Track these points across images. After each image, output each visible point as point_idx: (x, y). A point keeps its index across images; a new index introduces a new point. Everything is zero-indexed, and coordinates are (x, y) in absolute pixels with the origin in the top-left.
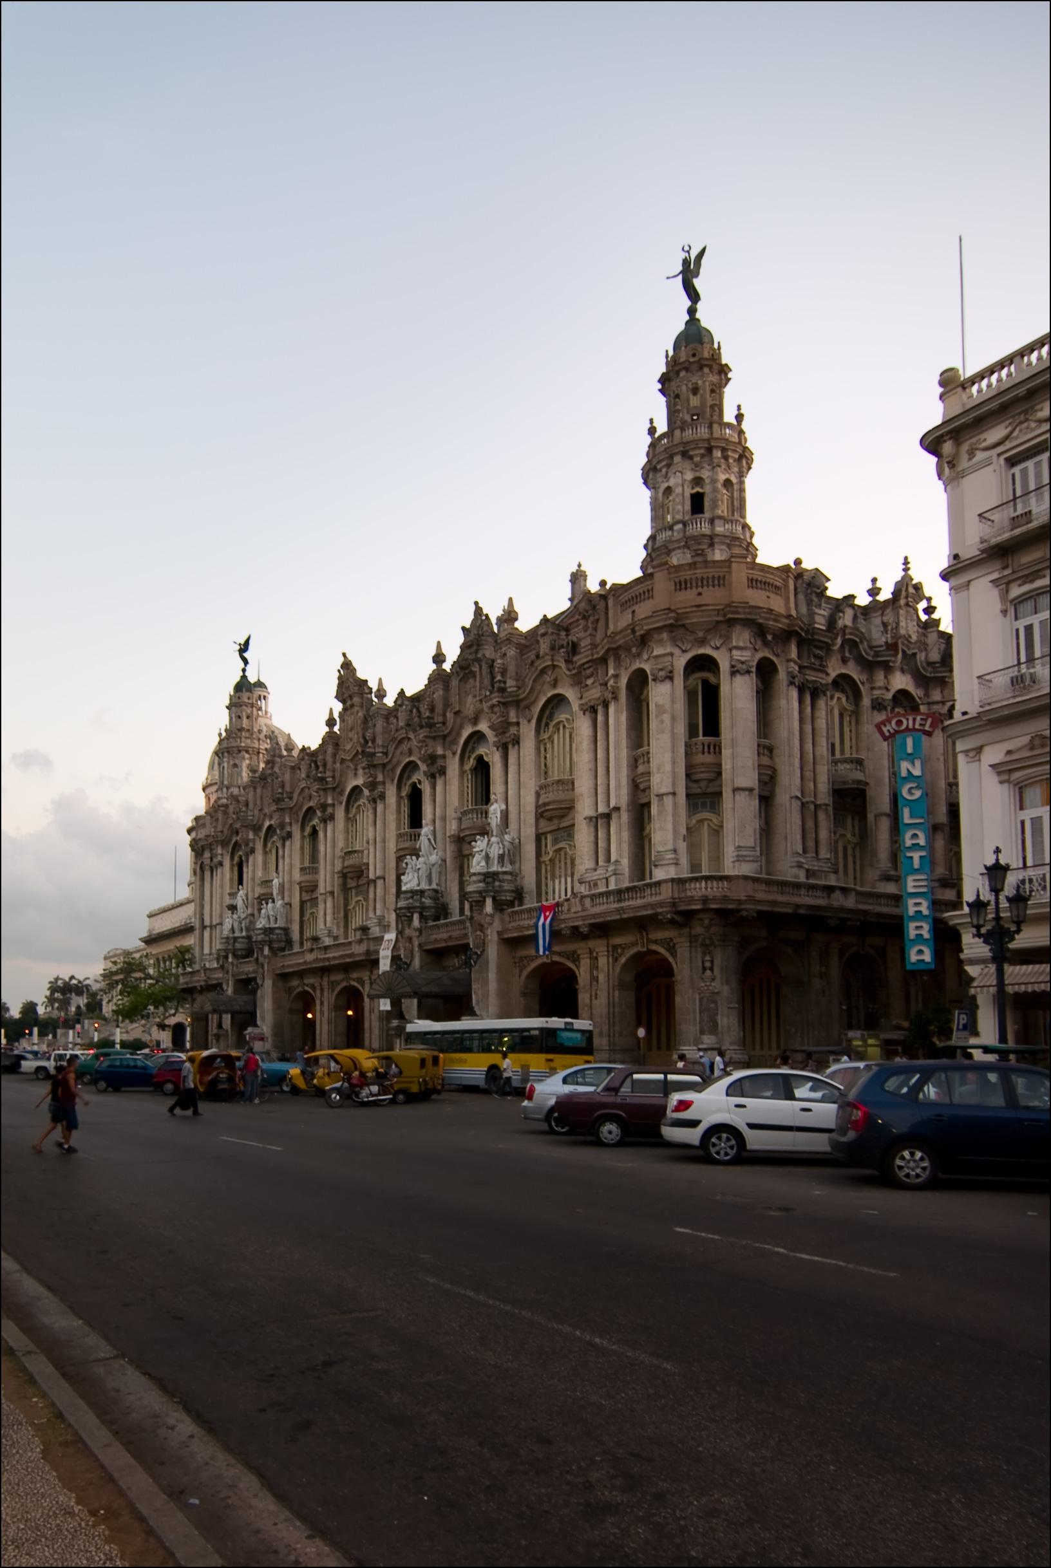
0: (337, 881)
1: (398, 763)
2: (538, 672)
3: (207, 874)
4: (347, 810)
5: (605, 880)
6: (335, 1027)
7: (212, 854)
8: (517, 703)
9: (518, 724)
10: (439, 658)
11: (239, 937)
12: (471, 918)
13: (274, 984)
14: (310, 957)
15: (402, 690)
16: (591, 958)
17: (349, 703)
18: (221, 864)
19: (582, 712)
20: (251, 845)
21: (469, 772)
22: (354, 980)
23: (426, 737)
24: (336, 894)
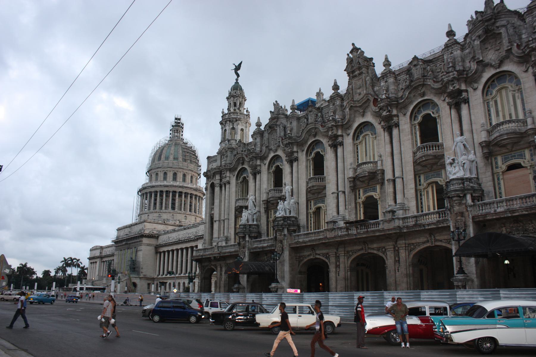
1: (411, 103)
3: (217, 189)
7: (221, 177)
10: (451, 33)
13: (290, 255)
14: (329, 235)
15: (415, 56)
17: (357, 73)
18: (229, 183)
19: (382, 130)
20: (258, 168)
22: (373, 249)
23: (454, 78)
24: (346, 193)
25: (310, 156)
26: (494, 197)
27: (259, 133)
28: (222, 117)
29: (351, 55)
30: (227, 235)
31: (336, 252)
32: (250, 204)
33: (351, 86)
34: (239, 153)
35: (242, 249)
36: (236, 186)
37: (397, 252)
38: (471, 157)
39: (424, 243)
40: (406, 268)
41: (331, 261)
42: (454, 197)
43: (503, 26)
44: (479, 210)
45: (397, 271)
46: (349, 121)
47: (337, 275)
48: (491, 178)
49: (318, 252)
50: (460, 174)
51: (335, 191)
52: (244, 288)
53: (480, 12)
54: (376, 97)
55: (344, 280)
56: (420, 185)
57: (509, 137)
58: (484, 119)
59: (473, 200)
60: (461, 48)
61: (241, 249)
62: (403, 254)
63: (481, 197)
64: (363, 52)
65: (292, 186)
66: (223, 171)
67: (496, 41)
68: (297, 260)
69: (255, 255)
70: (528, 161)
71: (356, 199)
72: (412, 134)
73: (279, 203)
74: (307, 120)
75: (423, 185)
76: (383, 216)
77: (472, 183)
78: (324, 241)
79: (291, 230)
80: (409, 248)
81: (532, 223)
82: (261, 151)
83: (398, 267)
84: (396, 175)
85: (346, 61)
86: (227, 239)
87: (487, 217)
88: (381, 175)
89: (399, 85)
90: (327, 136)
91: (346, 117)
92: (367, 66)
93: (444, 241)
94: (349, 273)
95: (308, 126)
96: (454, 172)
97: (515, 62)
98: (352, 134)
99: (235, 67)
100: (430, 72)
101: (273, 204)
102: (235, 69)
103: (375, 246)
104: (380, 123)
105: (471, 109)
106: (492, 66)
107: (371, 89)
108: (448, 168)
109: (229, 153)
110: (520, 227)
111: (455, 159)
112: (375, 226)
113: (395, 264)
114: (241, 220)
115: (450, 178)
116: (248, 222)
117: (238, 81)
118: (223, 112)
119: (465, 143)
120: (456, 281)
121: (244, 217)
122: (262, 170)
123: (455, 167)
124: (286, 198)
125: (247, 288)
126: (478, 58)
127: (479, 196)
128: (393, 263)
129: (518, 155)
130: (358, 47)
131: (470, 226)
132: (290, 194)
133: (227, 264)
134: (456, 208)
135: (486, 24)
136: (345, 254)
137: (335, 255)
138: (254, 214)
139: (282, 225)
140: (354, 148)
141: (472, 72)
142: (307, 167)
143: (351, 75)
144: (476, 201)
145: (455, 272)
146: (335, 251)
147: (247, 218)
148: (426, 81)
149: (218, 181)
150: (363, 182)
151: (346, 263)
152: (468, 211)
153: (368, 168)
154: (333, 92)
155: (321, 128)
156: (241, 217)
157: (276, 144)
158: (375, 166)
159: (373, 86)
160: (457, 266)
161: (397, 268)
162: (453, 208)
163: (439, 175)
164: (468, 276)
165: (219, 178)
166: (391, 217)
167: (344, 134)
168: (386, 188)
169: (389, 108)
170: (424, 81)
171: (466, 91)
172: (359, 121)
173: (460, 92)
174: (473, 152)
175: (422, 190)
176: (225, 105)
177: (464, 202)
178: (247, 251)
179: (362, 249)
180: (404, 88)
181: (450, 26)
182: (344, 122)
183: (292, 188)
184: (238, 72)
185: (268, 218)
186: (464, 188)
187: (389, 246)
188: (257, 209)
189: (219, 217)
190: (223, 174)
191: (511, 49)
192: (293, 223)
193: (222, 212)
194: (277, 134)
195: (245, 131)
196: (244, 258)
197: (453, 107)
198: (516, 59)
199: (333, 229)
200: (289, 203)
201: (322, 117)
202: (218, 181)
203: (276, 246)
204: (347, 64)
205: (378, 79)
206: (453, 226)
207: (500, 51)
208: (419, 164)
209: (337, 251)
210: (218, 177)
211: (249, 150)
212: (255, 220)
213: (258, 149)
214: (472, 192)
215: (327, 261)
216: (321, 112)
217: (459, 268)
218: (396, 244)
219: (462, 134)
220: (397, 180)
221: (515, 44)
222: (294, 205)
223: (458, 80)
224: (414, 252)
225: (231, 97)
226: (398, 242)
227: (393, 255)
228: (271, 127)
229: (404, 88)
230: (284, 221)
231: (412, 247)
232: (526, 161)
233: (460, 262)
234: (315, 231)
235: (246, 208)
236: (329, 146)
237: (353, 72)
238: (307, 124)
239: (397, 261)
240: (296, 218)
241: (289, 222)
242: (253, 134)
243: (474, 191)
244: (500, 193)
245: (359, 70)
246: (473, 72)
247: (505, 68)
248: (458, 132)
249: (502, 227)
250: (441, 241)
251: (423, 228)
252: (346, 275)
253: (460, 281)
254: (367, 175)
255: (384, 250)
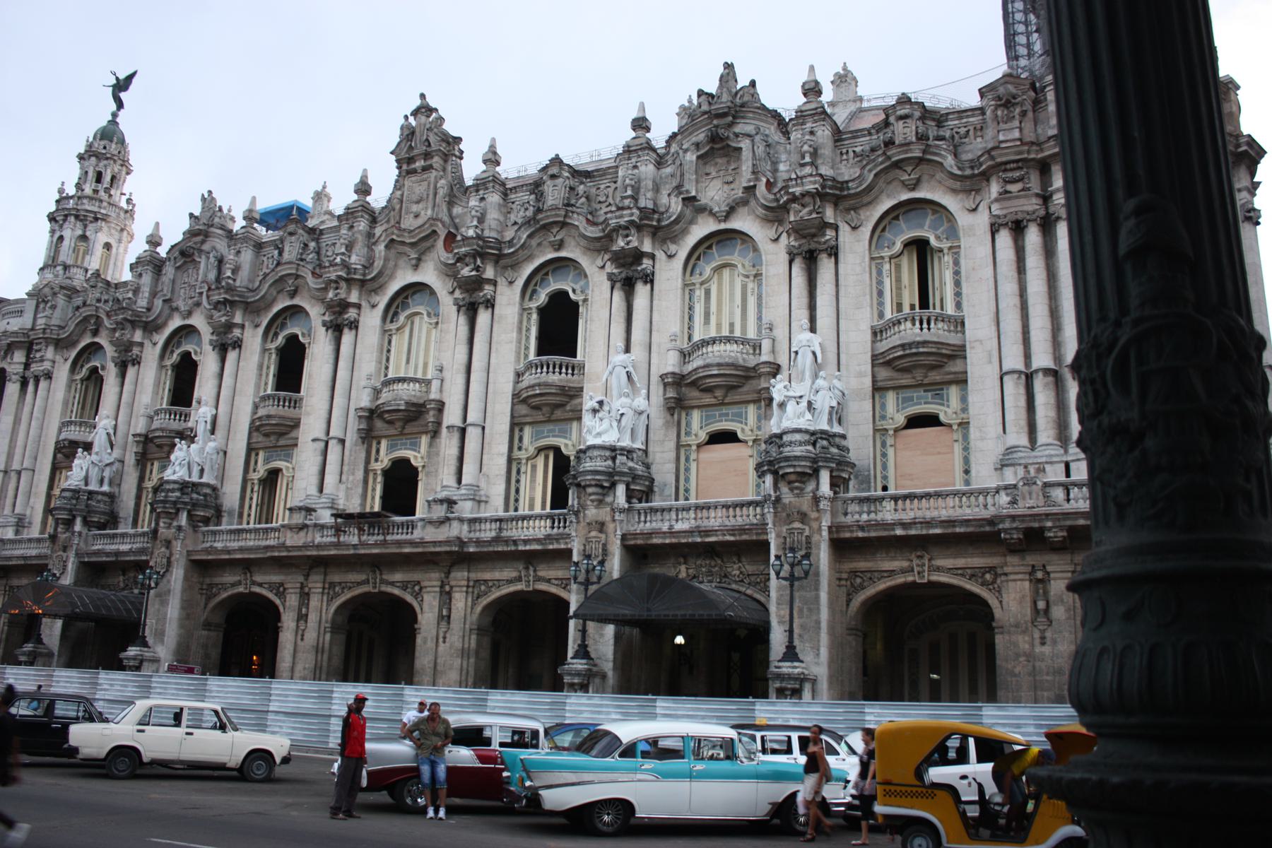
0: (354, 425)
1: (530, 258)
2: (887, 164)
4: (384, 319)
5: (1063, 466)
6: (330, 659)
7: (28, 357)
8: (837, 201)
9: (836, 228)
10: (641, 124)
11: (97, 493)
12: (778, 500)
13: (186, 578)
14: (292, 539)
15: (557, 155)
16: (1031, 581)
17: (419, 164)
18: (49, 376)
19: (455, 308)
20: (136, 350)
21: (169, 368)
22: (392, 584)
23: (632, 222)
24: (347, 444)
25: (272, 341)
26: (673, 497)
27: (151, 264)
28: (57, 201)
29: (412, 120)
30: (22, 512)
31: (302, 583)
32: (99, 438)
33: (399, 193)
34: (88, 302)
35: (61, 553)
36: (69, 387)
37: (446, 596)
38: (640, 402)
39: (510, 582)
40: (464, 636)
41: (287, 604)
42: (590, 486)
43: (749, 136)
44: (639, 522)
45: (441, 640)
46: (380, 274)
47: (299, 637)
48: (673, 455)
49: (258, 578)
50: (610, 438)
51: (322, 436)
52: (50, 655)
53: (707, 94)
54: (452, 230)
55: (314, 653)
56: (520, 449)
57: (722, 372)
58: (678, 325)
59: (629, 498)
60: (656, 161)
61: (56, 552)
62: (460, 602)
63: (647, 494)
64: (441, 119)
65: (217, 409)
66: (37, 344)
67: (728, 162)
68: (202, 594)
69: (94, 571)
70: (752, 431)
71: (367, 462)
72: (520, 329)
73: (175, 445)
74: (280, 254)
75: (526, 450)
76: (426, 510)
77: (632, 460)
78: (276, 554)
79: (198, 518)
80: (476, 590)
81: (740, 561)
82: (149, 310)
83: (446, 632)
84: (469, 420)
85: (398, 132)
86: (21, 524)
87: (652, 538)
88: (436, 412)
89: (509, 213)
90: (322, 301)
91: (376, 264)
92: (446, 155)
93: (556, 582)
94: (328, 636)
95: (279, 268)
96: (598, 430)
97: (758, 216)
98: (382, 306)
99: (115, 82)
100: (583, 200)
101: (160, 446)
102: (114, 86)
103: (398, 577)
104: (452, 293)
105: (655, 296)
106: (712, 213)
107: (445, 210)
108: (587, 419)
109: (61, 300)
110: (715, 566)
111: (605, 402)
112: (405, 531)
113: (438, 624)
114: (67, 478)
115: (589, 443)
116: (86, 484)
117: (118, 120)
118: (61, 191)
119: (631, 369)
120: (570, 674)
121: (79, 470)
122: (143, 356)
123: (601, 420)
124: (195, 436)
125: (59, 656)
126: (687, 191)
127: (643, 492)
128: (436, 622)
129: (735, 415)
130: (432, 103)
131: (614, 555)
132: (209, 427)
133: (11, 587)
134: (592, 513)
135: (715, 122)
136: (324, 588)
137: (298, 590)
138: (107, 465)
139: (175, 503)
140: (383, 339)
141: (670, 217)
142: (260, 367)
143: (405, 167)
144: (635, 500)
145: (570, 653)
146: (301, 579)
147: (84, 473)
148: (570, 218)
149: (17, 366)
150: (390, 422)
151: (324, 611)
152: (614, 521)
153: (408, 392)
154: (355, 197)
155: (310, 279)
156: (70, 468)
157: (191, 298)
158: (424, 389)
159: (451, 204)
160: (575, 641)
161: (441, 635)
162: (585, 509)
163: (565, 432)
164: (595, 665)
165: (23, 360)
166: (443, 514)
167: (364, 304)
168: (443, 445)
169: (479, 262)
170: (566, 216)
171: (652, 257)
172: (405, 277)
173: (638, 256)
174: (644, 392)
175: (524, 461)
176: (69, 175)
177: (609, 499)
178: (72, 559)
179: (366, 582)
180: (520, 221)
181: (642, 107)
182: (369, 274)
183: (214, 412)
184: (123, 95)
185: (141, 479)
186: (614, 469)
187: (431, 580)
188: (117, 453)
189: (7, 463)
190: (37, 351)
191: (755, 186)
192: (205, 500)
193: (18, 451)
194: (198, 274)
195: (114, 250)
196: (63, 577)
197: (618, 285)
198: (760, 211)
199: (304, 527)
200: (202, 450)
201: (318, 253)
202: (20, 369)
203: (152, 553)
204: (398, 140)
205: (466, 189)
206: (579, 550)
207: (732, 186)
208: (524, 401)
209: (306, 580)
210: (19, 357)
211: (118, 300)
212: (106, 481)
213: (142, 303)
214: (630, 479)
215: (278, 602)
216: (317, 240)
217: (579, 645)
218: (447, 577)
219: (627, 350)
220: (470, 430)
221: (764, 180)
222: (214, 457)
223: (639, 228)
224: (485, 601)
225: (90, 156)
226: (453, 575)
227: (436, 603)
228: (186, 253)
229: (520, 221)
230: (183, 494)
231: (483, 588)
232: (747, 429)
233: (584, 631)
234: (258, 526)
235: (88, 447)
236: (324, 324)
237: (411, 160)
238: (278, 264)
239: (445, 619)
240: (214, 489)
241: (195, 496)
242: (137, 263)
243: (633, 478)
244: (687, 490)
245: (425, 160)
246: (672, 219)
247: (736, 224)
248: (621, 345)
249: (680, 564)
250: (549, 581)
251: (513, 548)
252: (321, 639)
253: (578, 674)
254: (403, 408)
255: (417, 588)
